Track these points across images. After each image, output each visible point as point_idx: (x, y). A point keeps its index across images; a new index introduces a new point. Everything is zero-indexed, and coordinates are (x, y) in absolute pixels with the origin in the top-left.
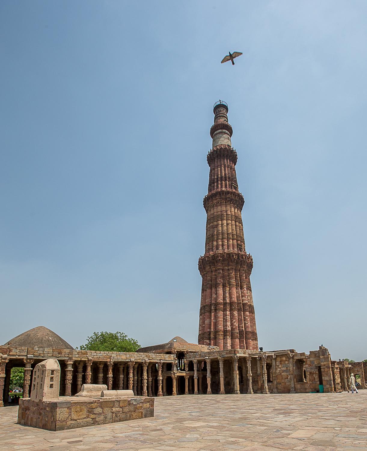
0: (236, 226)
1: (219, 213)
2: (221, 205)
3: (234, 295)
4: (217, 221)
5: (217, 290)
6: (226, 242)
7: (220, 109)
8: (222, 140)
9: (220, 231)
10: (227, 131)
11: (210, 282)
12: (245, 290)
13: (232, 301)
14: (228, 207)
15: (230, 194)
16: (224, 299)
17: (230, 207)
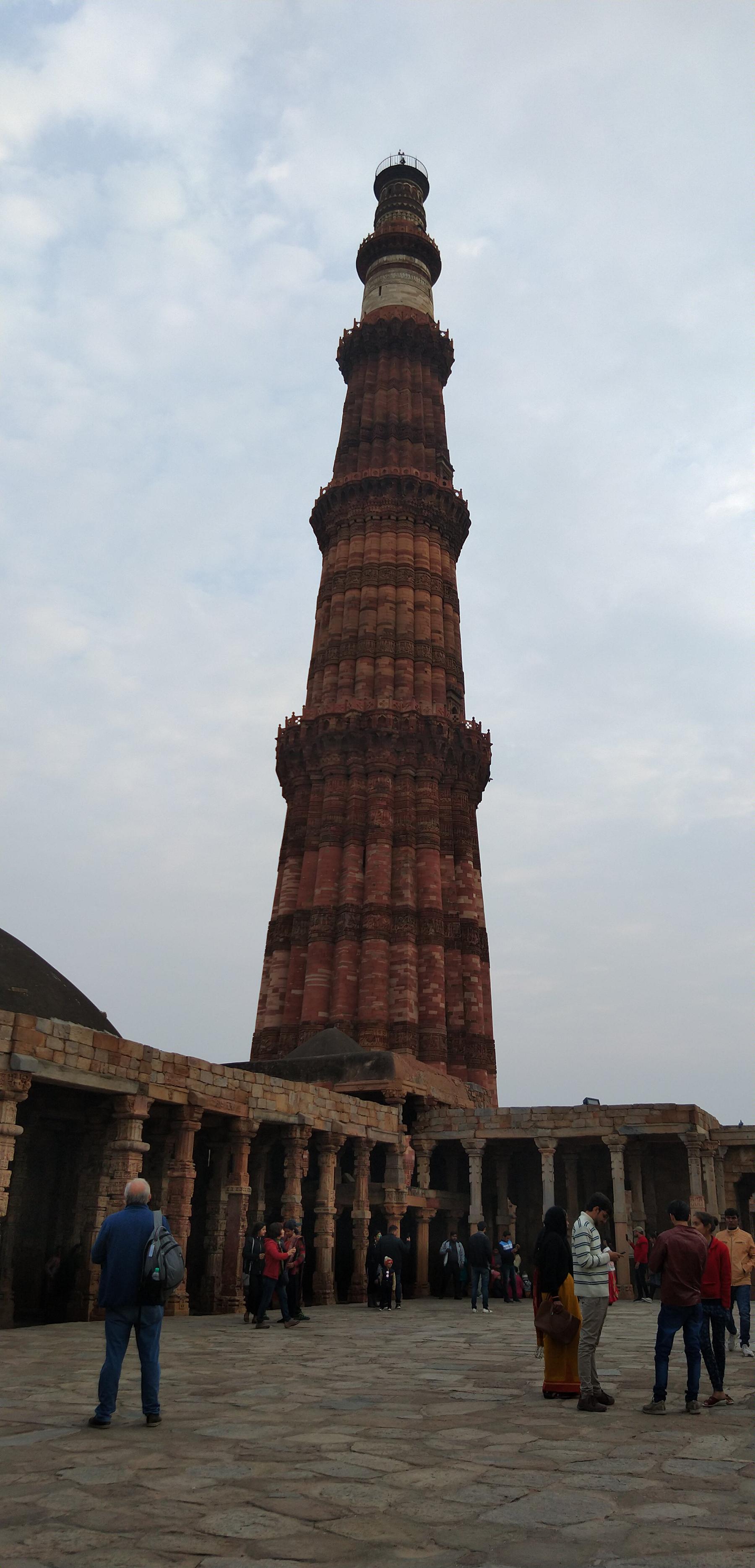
0: (446, 618)
1: (388, 558)
2: (398, 528)
3: (436, 883)
4: (378, 587)
5: (370, 853)
6: (409, 673)
7: (401, 188)
8: (409, 293)
9: (390, 624)
10: (425, 267)
11: (338, 819)
12: (469, 871)
13: (426, 906)
14: (423, 541)
15: (434, 496)
16: (395, 892)
17: (430, 545)
